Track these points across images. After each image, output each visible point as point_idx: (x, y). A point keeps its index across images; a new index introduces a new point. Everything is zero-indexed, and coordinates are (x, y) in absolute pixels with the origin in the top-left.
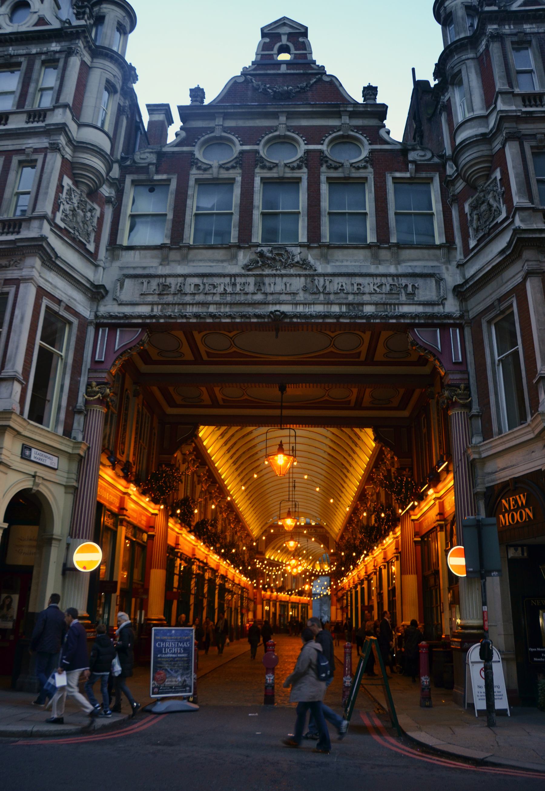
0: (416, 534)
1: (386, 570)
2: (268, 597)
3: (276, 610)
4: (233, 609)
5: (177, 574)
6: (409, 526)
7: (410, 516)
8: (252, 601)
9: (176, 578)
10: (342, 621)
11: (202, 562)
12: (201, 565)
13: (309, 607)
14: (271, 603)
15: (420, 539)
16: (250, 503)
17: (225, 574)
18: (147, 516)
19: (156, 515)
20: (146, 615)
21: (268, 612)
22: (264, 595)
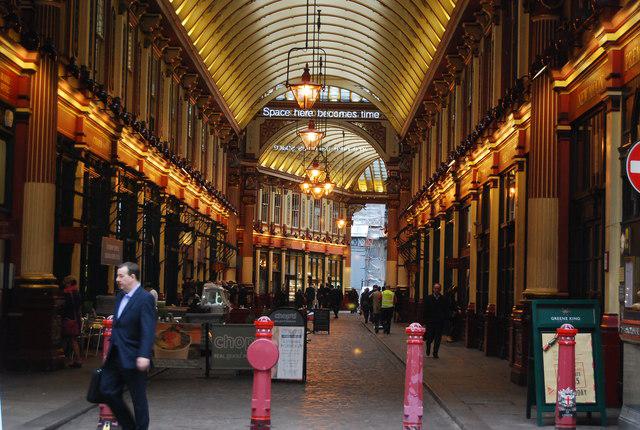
0: (562, 118)
1: (498, 190)
4: (196, 264)
5: (79, 194)
6: (549, 102)
7: (552, 81)
8: (234, 249)
9: (78, 201)
10: (408, 288)
11: (131, 170)
12: (129, 175)
14: (271, 253)
15: (569, 128)
16: (229, 57)
17: (178, 196)
18: (12, 75)
19: (31, 72)
20: (17, 271)
21: (265, 272)
22: (257, 238)
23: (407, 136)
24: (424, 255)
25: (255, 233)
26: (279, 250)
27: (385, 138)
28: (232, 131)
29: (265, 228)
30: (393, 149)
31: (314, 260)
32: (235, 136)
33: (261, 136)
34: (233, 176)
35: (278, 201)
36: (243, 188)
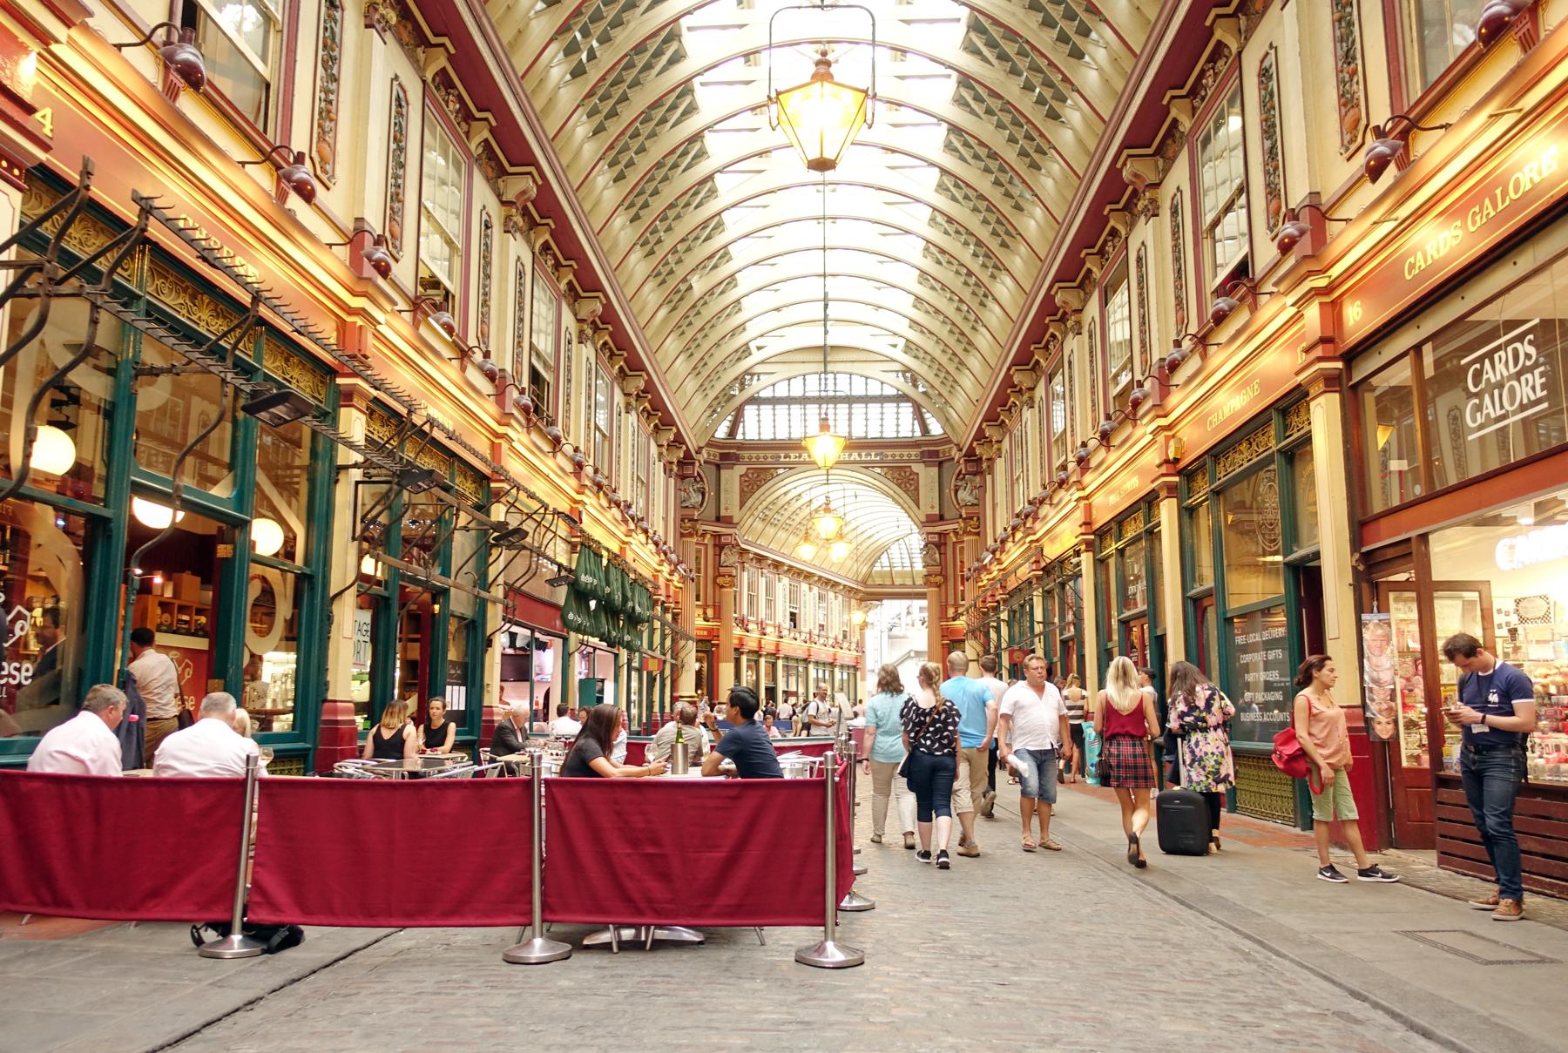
2: (753, 645)
3: (774, 679)
13: (859, 674)
14: (762, 661)
22: (741, 639)
23: (980, 436)
24: (1046, 622)
25: (738, 631)
26: (774, 655)
27: (917, 489)
28: (679, 440)
29: (751, 626)
30: (929, 501)
31: (821, 675)
32: (688, 454)
33: (742, 491)
34: (687, 524)
35: (769, 589)
36: (718, 565)
